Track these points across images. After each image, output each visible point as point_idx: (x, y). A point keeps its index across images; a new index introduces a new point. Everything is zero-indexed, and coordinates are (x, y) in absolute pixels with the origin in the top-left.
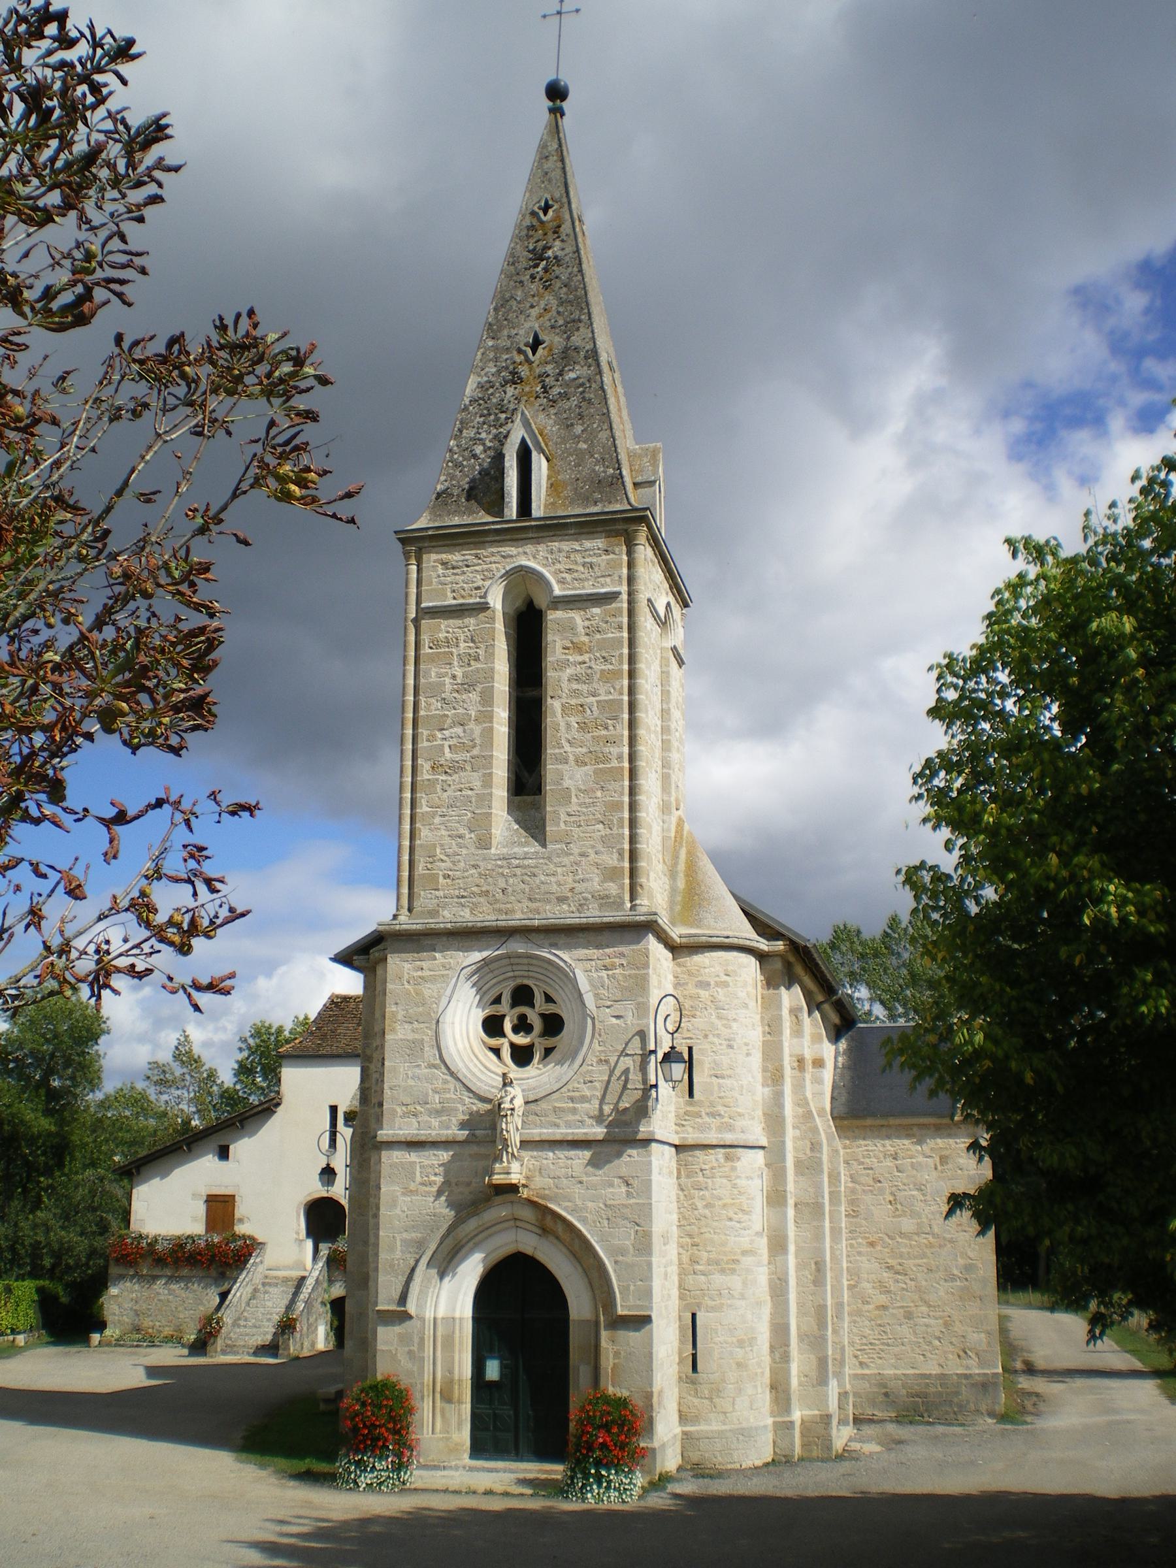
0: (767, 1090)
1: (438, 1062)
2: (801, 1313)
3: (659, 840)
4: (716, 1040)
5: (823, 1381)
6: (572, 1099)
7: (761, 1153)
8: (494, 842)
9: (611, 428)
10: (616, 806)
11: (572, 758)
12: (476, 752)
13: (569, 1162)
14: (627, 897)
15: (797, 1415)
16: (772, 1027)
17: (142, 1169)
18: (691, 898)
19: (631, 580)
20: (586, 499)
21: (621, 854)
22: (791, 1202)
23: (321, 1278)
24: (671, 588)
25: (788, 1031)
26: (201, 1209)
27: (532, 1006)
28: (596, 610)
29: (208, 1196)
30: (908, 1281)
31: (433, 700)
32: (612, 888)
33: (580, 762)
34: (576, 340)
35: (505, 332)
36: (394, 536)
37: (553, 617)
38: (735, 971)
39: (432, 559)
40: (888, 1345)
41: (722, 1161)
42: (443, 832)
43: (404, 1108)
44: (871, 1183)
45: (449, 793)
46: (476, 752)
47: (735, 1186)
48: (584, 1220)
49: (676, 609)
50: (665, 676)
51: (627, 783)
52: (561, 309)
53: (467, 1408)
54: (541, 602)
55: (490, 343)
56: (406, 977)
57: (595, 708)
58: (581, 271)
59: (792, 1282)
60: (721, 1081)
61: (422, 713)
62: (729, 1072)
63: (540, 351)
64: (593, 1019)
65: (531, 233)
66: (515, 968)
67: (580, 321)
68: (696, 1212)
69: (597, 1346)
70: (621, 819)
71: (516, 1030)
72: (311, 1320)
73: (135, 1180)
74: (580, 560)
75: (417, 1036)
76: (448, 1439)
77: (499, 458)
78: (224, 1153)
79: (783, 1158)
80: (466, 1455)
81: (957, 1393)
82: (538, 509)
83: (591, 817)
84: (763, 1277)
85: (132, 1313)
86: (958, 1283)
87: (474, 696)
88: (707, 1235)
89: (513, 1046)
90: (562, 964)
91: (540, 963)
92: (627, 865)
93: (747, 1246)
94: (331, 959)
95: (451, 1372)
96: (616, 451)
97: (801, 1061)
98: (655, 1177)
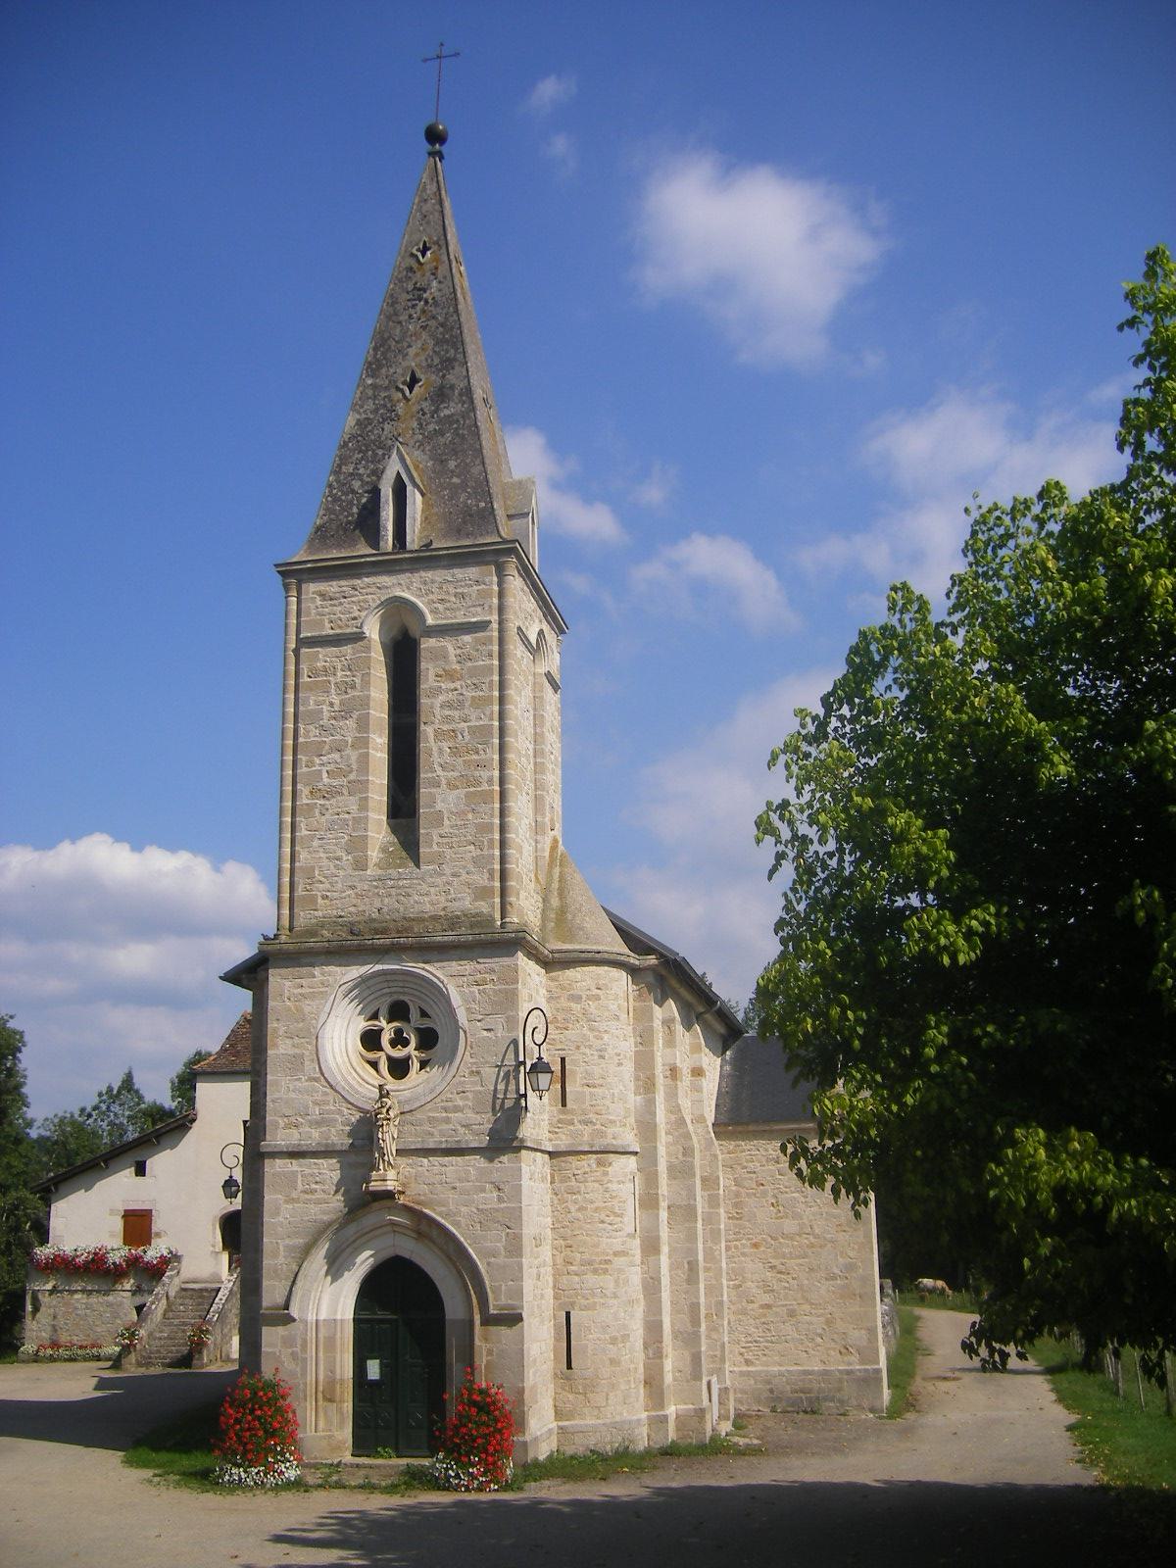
0: (638, 1098)
1: (319, 1075)
2: (676, 1310)
3: (531, 859)
4: (587, 1051)
5: (696, 1376)
6: (446, 1110)
7: (633, 1159)
8: (371, 864)
9: (483, 463)
10: (486, 828)
11: (444, 782)
12: (352, 777)
13: (443, 1169)
14: (497, 916)
15: (671, 1410)
16: (645, 1038)
17: (62, 1188)
18: (561, 918)
19: (501, 609)
20: (458, 532)
21: (491, 873)
22: (664, 1204)
23: (235, 1289)
24: (545, 616)
25: (661, 1041)
26: (118, 1225)
27: (408, 1020)
28: (467, 638)
29: (126, 1211)
30: (791, 1281)
31: (311, 727)
32: (483, 907)
33: (452, 786)
34: (451, 378)
35: (384, 370)
36: (274, 569)
37: (427, 644)
38: (606, 985)
39: (311, 588)
40: (772, 1342)
41: (594, 1166)
42: (322, 855)
43: (285, 1120)
44: (754, 1186)
45: (327, 816)
46: (352, 777)
47: (606, 1190)
48: (457, 1224)
49: (551, 637)
50: (538, 701)
51: (497, 805)
52: (437, 349)
53: (348, 1406)
54: (415, 630)
55: (369, 382)
56: (287, 994)
57: (466, 734)
58: (456, 311)
59: (665, 1281)
60: (591, 1089)
61: (301, 740)
62: (601, 1081)
63: (416, 389)
64: (465, 1032)
65: (410, 274)
66: (391, 984)
67: (455, 359)
68: (569, 1216)
69: (472, 1340)
70: (491, 841)
71: (394, 1043)
72: (226, 1330)
73: (53, 1198)
74: (452, 590)
75: (297, 1051)
76: (330, 1437)
77: (375, 493)
78: (141, 1170)
79: (655, 1163)
80: (348, 1453)
81: (840, 1390)
82: (414, 538)
83: (462, 838)
84: (635, 1277)
85: (49, 1328)
86: (839, 1282)
87: (351, 723)
88: (580, 1238)
89: (390, 1059)
90: (435, 980)
91: (415, 980)
92: (497, 884)
93: (619, 1248)
94: (221, 978)
95: (333, 1372)
96: (488, 485)
97: (673, 1072)
98: (525, 1182)
